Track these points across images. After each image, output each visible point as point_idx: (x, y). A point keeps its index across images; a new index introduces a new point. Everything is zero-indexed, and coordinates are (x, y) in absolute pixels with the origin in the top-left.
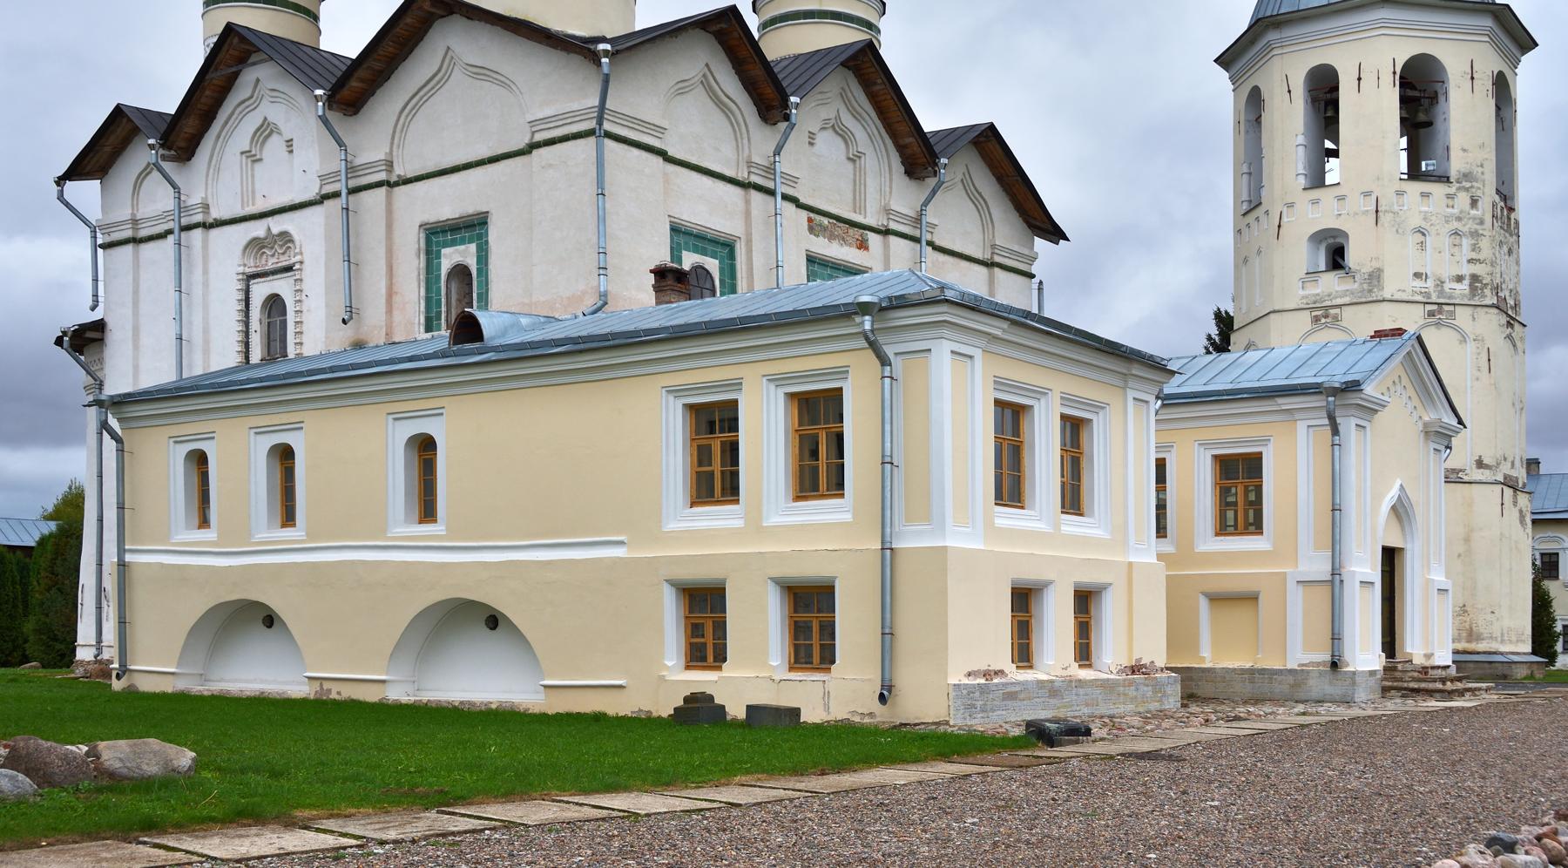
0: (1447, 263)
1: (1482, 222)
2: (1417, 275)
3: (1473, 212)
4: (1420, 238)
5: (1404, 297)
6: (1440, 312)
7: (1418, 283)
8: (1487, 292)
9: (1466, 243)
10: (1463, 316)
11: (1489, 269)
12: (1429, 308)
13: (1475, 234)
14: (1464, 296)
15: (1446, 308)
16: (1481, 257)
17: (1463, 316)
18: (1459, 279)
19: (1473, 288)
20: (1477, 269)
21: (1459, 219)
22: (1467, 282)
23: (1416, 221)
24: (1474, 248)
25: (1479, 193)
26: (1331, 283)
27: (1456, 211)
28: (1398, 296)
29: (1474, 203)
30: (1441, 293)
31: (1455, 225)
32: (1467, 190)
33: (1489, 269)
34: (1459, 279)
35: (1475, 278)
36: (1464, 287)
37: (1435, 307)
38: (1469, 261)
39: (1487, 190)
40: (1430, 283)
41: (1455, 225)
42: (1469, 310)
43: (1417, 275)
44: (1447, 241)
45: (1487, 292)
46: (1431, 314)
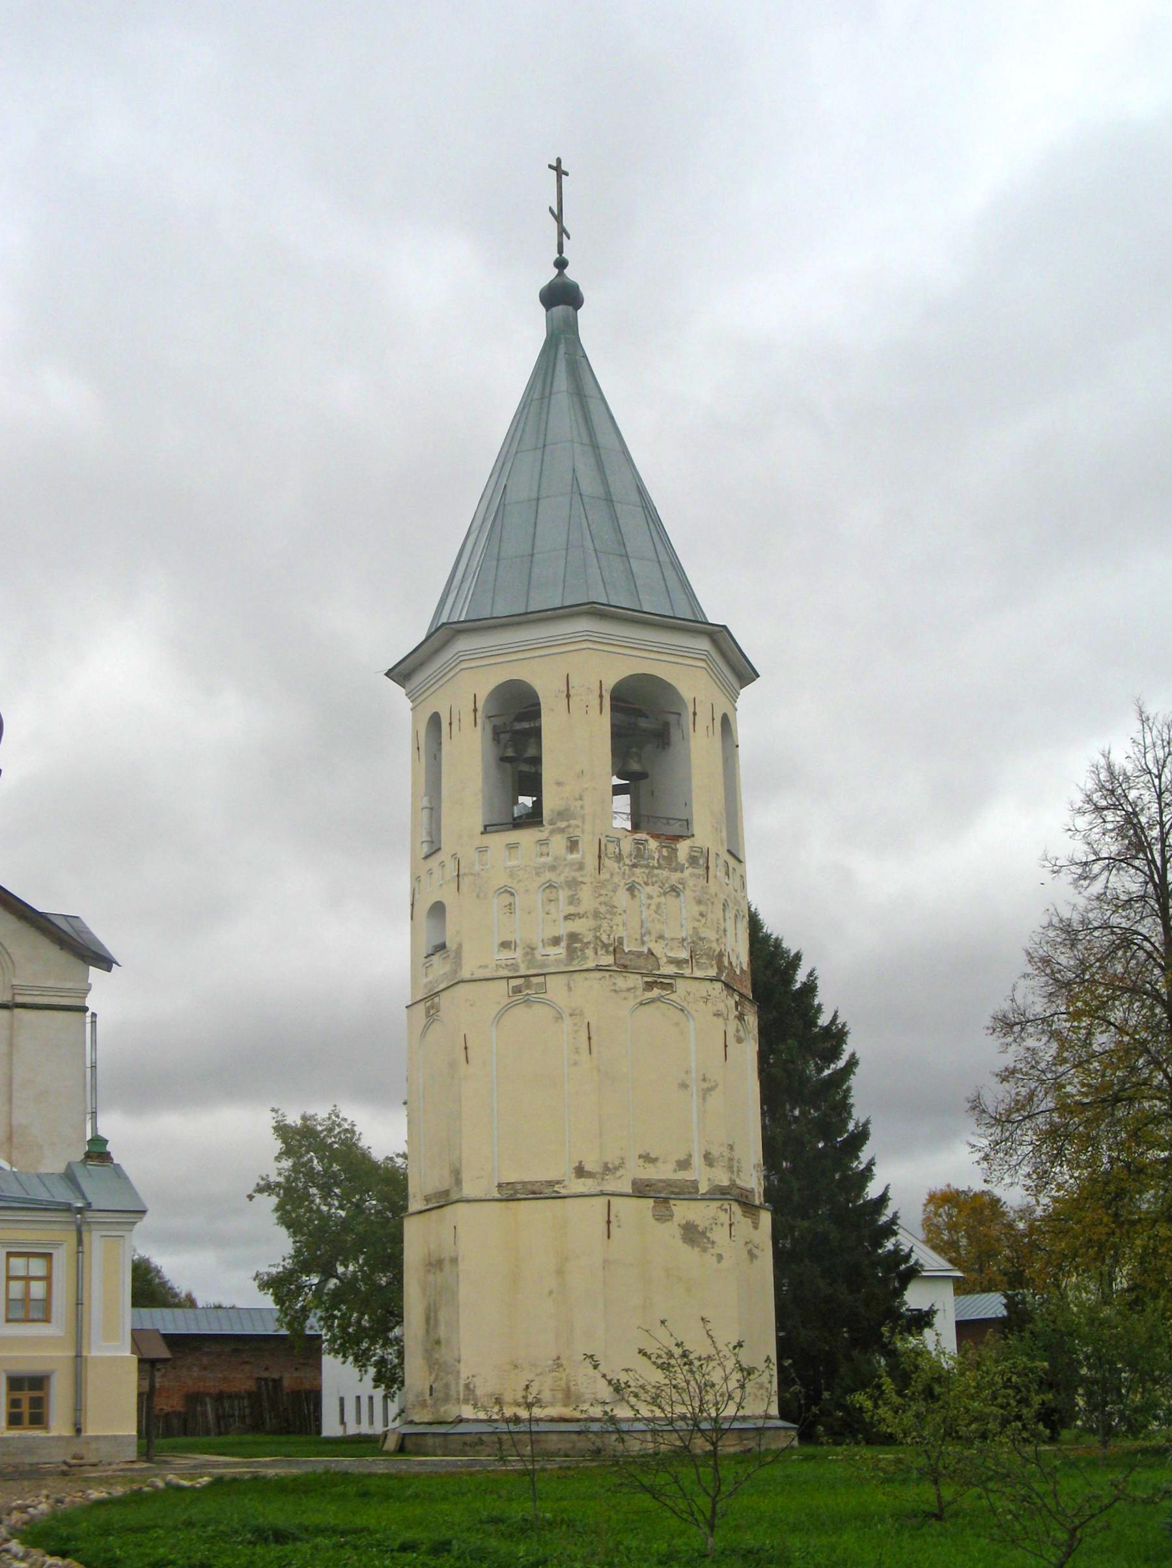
0: (539, 924)
1: (581, 867)
2: (505, 945)
3: (570, 857)
4: (507, 899)
5: (488, 974)
6: (528, 987)
7: (506, 954)
8: (589, 952)
9: (563, 895)
10: (556, 985)
11: (591, 923)
12: (514, 983)
13: (573, 884)
14: (558, 961)
15: (534, 980)
16: (581, 910)
17: (556, 985)
18: (556, 941)
19: (571, 951)
20: (576, 926)
21: (553, 868)
22: (563, 944)
23: (502, 880)
24: (573, 900)
25: (578, 832)
26: (440, 967)
27: (548, 860)
28: (480, 974)
29: (573, 845)
30: (531, 962)
31: (548, 875)
32: (562, 831)
33: (591, 923)
34: (556, 941)
35: (573, 937)
36: (560, 951)
37: (521, 981)
38: (567, 918)
39: (588, 827)
40: (518, 954)
41: (548, 875)
42: (562, 979)
43: (505, 945)
44: (539, 897)
45: (589, 952)
46: (517, 990)
